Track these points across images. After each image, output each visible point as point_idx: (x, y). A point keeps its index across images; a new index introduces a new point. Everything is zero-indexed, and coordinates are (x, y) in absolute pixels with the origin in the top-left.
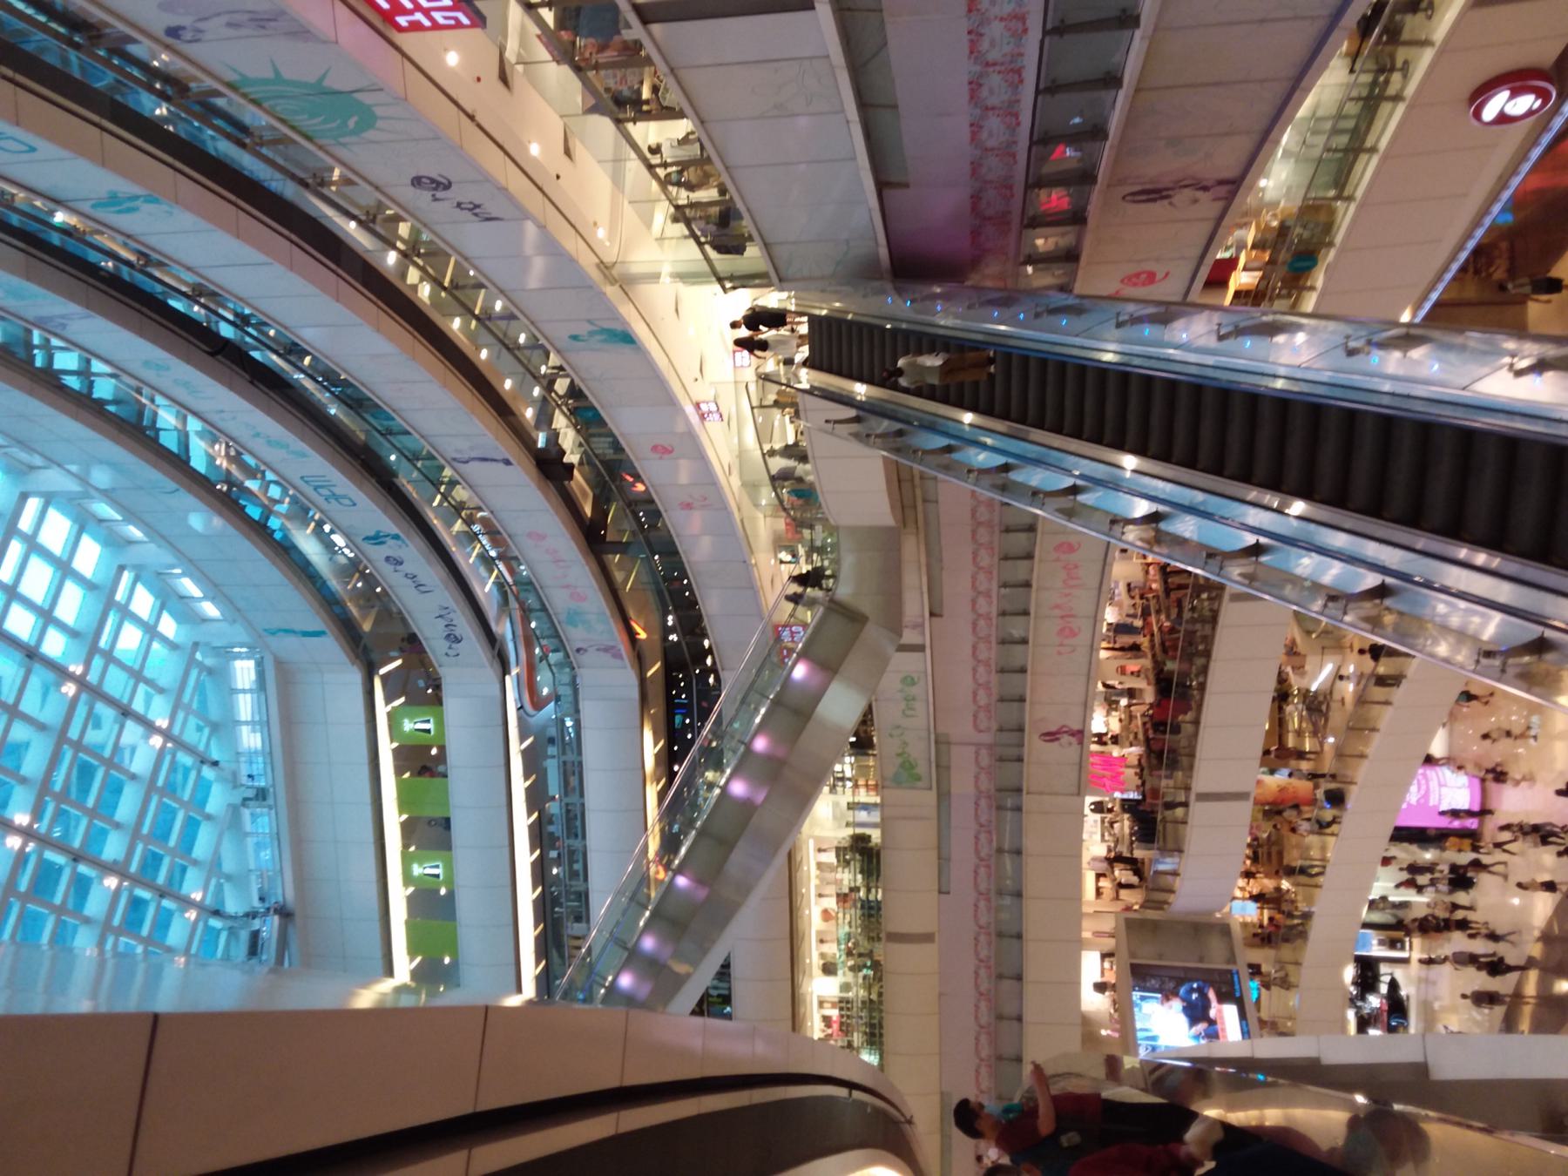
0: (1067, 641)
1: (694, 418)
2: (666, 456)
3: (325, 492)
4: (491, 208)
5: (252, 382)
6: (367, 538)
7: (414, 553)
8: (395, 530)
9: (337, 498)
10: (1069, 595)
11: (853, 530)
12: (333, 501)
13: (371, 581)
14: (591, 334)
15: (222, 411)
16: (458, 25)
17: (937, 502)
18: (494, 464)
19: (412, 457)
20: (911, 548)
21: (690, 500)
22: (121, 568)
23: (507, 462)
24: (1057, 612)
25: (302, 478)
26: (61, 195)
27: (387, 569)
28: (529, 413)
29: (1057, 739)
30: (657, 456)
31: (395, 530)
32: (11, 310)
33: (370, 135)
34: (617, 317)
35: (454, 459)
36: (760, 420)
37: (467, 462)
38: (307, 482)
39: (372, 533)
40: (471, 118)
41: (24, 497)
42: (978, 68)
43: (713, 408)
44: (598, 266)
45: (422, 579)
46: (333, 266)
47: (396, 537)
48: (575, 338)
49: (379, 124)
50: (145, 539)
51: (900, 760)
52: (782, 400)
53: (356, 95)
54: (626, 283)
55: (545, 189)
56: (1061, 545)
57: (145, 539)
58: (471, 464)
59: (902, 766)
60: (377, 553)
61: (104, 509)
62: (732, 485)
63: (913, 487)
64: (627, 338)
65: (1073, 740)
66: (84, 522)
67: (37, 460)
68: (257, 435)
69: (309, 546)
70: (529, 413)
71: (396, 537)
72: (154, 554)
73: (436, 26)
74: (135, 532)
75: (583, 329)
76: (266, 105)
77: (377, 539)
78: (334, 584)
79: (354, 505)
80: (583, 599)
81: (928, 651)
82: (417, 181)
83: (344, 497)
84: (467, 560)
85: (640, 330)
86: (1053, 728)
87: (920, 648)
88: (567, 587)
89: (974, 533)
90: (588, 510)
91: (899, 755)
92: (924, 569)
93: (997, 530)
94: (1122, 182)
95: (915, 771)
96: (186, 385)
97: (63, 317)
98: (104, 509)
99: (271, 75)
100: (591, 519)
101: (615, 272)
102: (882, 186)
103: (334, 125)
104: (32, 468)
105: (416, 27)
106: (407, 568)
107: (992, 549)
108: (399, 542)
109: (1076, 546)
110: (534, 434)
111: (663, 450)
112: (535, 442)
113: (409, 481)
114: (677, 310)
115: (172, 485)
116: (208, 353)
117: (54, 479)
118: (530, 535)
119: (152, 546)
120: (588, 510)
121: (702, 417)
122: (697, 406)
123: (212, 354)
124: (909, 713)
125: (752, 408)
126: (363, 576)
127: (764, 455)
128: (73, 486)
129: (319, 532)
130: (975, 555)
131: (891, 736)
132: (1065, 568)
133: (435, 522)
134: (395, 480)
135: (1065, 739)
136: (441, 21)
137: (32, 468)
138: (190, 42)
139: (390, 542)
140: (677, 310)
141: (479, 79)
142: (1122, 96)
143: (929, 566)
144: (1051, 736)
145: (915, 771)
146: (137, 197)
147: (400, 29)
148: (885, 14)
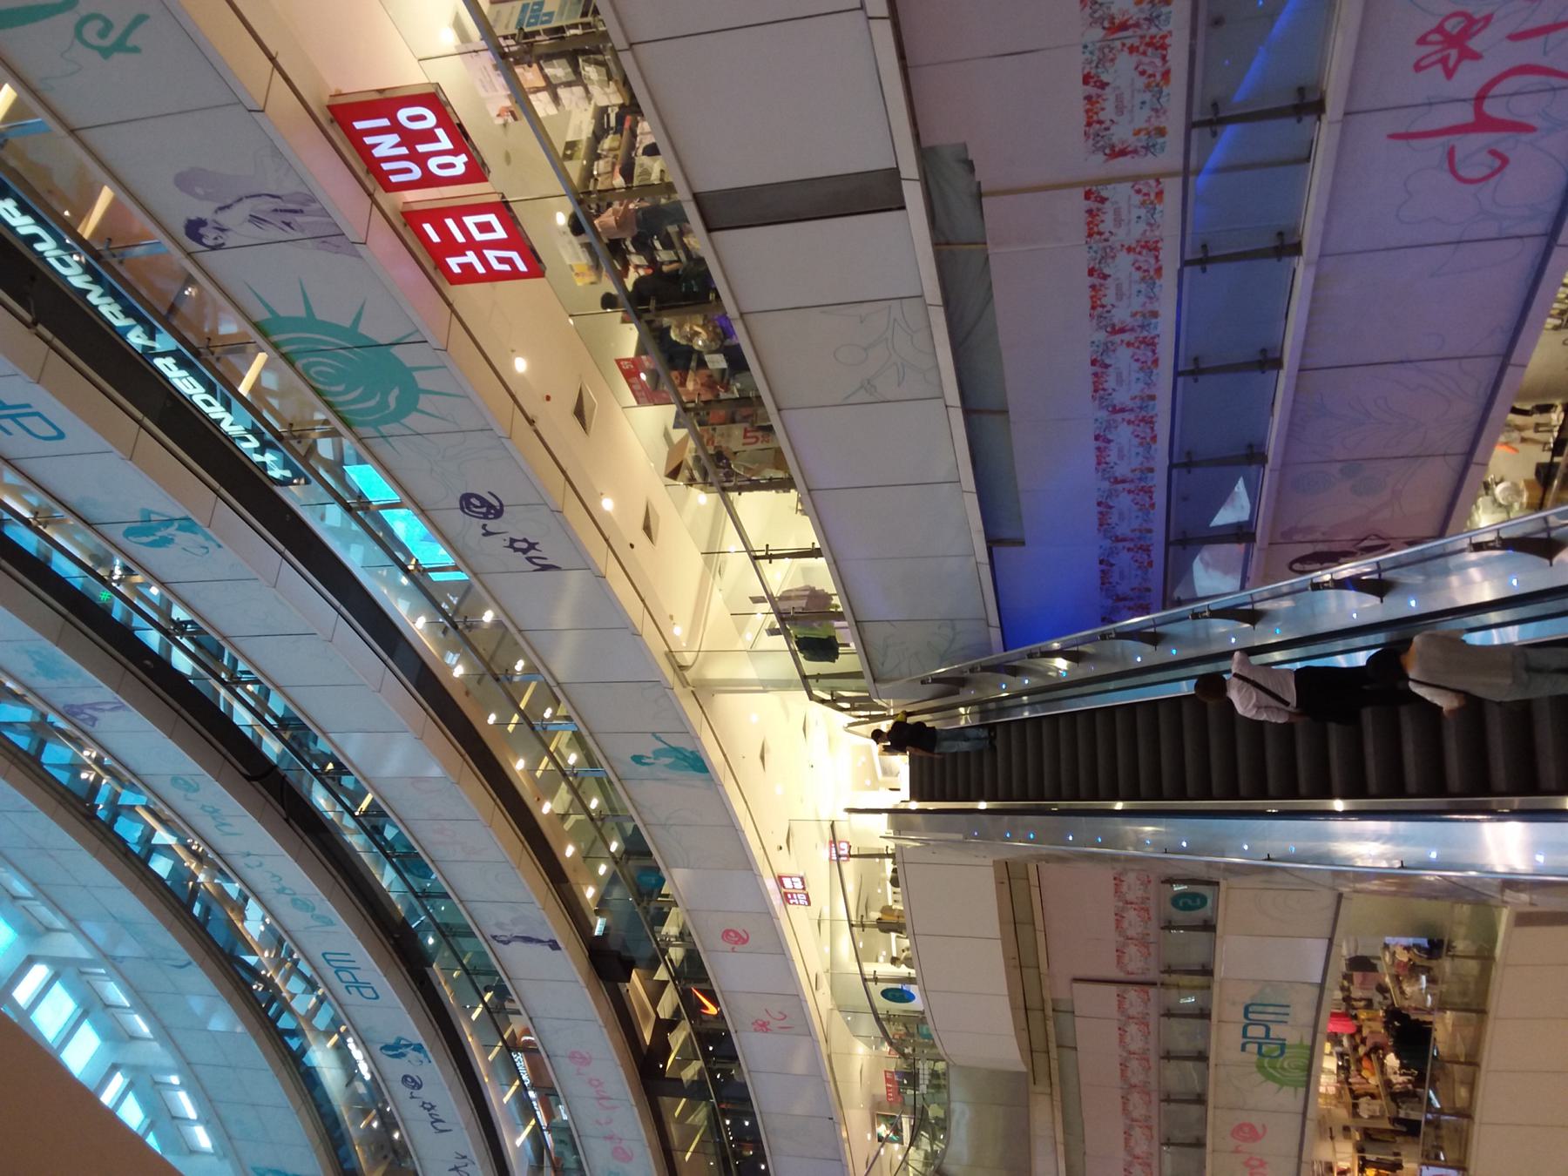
1: (776, 899)
2: (738, 948)
3: (345, 976)
4: (547, 551)
5: (287, 820)
6: (386, 1048)
7: (436, 1075)
8: (418, 1038)
9: (357, 985)
11: (968, 1072)
12: (353, 990)
13: (389, 1123)
14: (658, 754)
15: (249, 855)
16: (515, 274)
17: (1075, 1049)
18: (538, 947)
19: (447, 932)
20: (1044, 1117)
21: (766, 1018)
22: (114, 1068)
23: (554, 946)
25: (324, 955)
26: (94, 514)
27: (402, 1092)
28: (590, 893)
30: (729, 946)
31: (418, 1038)
32: (41, 692)
33: (413, 420)
34: (688, 731)
35: (494, 937)
36: (861, 945)
37: (506, 943)
38: (328, 961)
39: (391, 1041)
40: (531, 422)
41: (30, 961)
42: (1110, 602)
43: (799, 885)
44: (666, 655)
45: (440, 1112)
46: (385, 656)
47: (419, 1048)
48: (638, 759)
49: (424, 402)
50: (151, 1037)
52: (887, 919)
53: (395, 350)
54: (703, 691)
55: (611, 541)
56: (1240, 1127)
57: (151, 1037)
58: (513, 944)
60: (395, 1068)
61: (115, 993)
62: (820, 1002)
63: (1045, 1018)
64: (697, 763)
66: (91, 1007)
67: (59, 923)
68: (281, 891)
69: (321, 1058)
70: (590, 893)
71: (419, 1048)
72: (154, 1052)
73: (492, 276)
74: (141, 1026)
75: (647, 747)
76: (299, 364)
77: (395, 1049)
78: (345, 1115)
79: (377, 997)
80: (627, 1157)
82: (466, 501)
83: (367, 985)
84: (502, 1098)
85: (715, 757)
88: (610, 1138)
89: (1125, 1100)
90: (647, 1036)
92: (1061, 1148)
93: (1155, 1098)
94: (1288, 537)
96: (214, 813)
97: (93, 706)
98: (115, 993)
99: (300, 312)
100: (649, 1048)
101: (689, 675)
102: (992, 542)
103: (372, 403)
104: (49, 930)
105: (468, 274)
106: (424, 1094)
107: (1150, 1128)
108: (421, 1056)
109: (1260, 1131)
110: (592, 921)
111: (736, 938)
112: (592, 928)
113: (471, 1018)
114: (762, 758)
115: (185, 956)
116: (245, 776)
117: (69, 945)
118: (572, 1056)
119: (156, 1046)
120: (647, 1036)
121: (786, 898)
122: (780, 880)
123: (248, 779)
125: (851, 926)
126: (382, 1115)
127: (865, 980)
128: (82, 952)
129: (341, 1048)
130: (1128, 1134)
132: (1247, 1164)
133: (470, 1039)
134: (427, 969)
136: (496, 266)
137: (49, 930)
138: (213, 248)
139: (412, 1054)
140: (762, 758)
141: (548, 398)
142: (1285, 379)
143: (1066, 1145)
146: (171, 520)
147: (454, 279)
148: (989, 245)
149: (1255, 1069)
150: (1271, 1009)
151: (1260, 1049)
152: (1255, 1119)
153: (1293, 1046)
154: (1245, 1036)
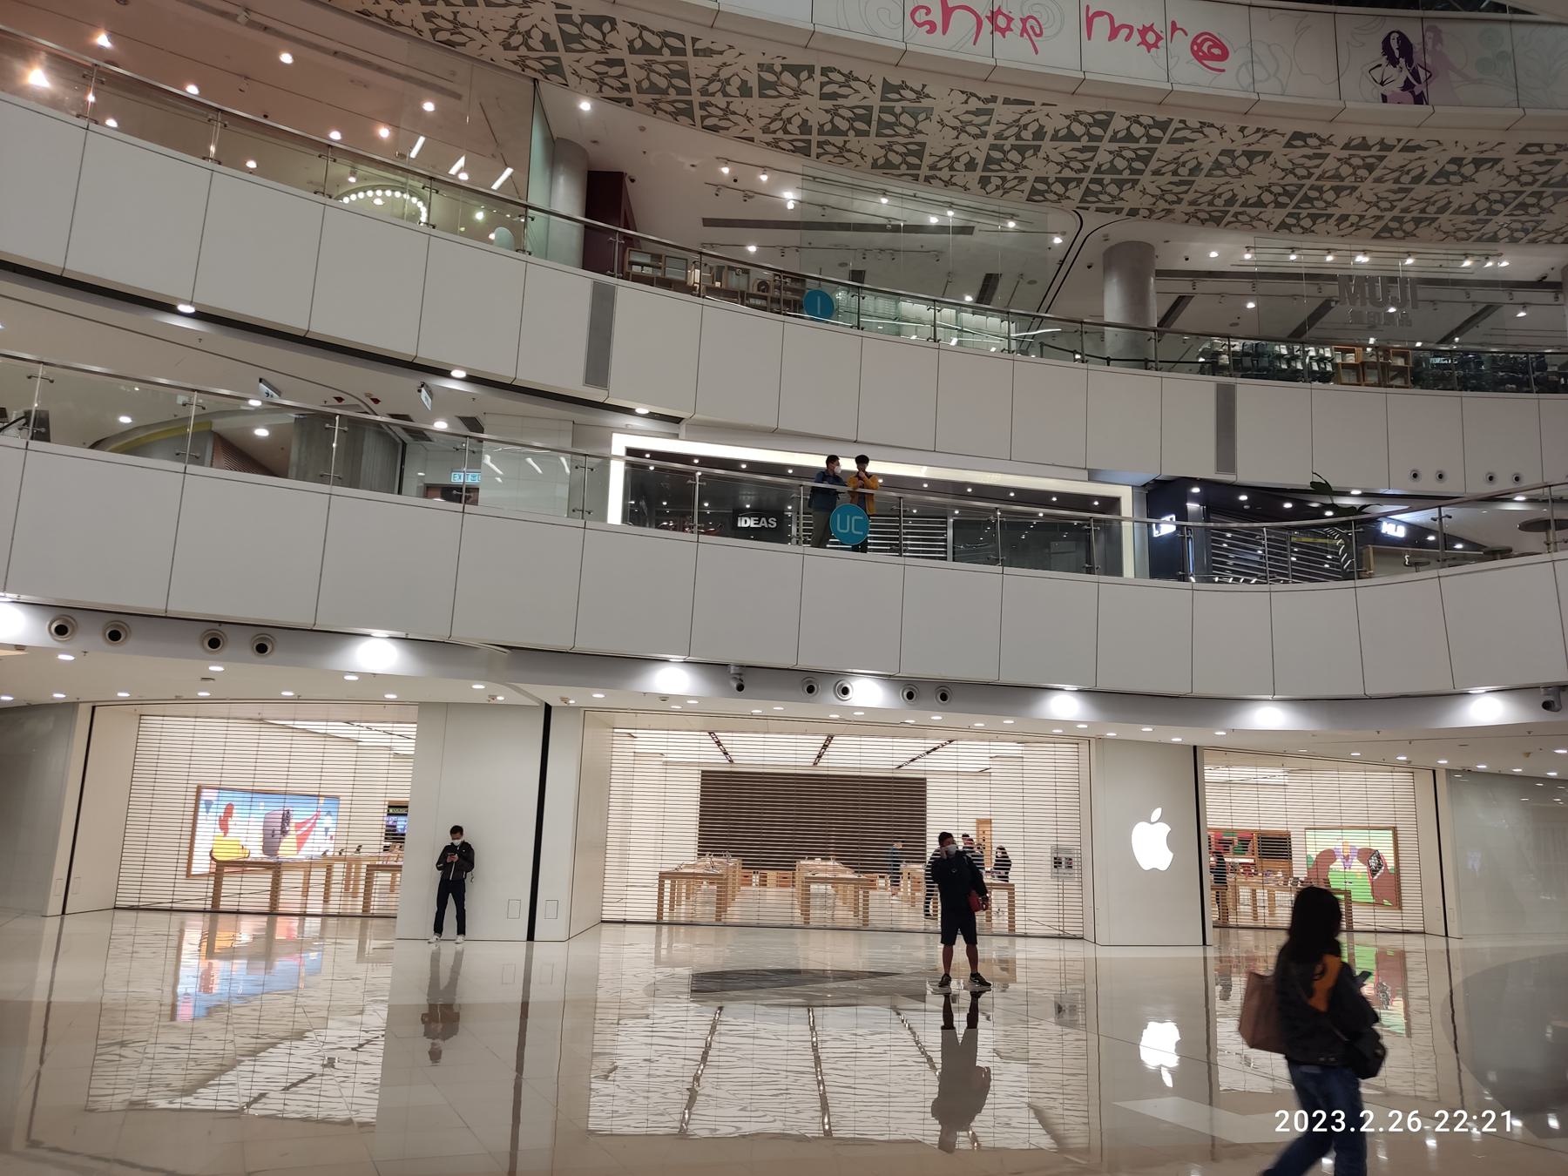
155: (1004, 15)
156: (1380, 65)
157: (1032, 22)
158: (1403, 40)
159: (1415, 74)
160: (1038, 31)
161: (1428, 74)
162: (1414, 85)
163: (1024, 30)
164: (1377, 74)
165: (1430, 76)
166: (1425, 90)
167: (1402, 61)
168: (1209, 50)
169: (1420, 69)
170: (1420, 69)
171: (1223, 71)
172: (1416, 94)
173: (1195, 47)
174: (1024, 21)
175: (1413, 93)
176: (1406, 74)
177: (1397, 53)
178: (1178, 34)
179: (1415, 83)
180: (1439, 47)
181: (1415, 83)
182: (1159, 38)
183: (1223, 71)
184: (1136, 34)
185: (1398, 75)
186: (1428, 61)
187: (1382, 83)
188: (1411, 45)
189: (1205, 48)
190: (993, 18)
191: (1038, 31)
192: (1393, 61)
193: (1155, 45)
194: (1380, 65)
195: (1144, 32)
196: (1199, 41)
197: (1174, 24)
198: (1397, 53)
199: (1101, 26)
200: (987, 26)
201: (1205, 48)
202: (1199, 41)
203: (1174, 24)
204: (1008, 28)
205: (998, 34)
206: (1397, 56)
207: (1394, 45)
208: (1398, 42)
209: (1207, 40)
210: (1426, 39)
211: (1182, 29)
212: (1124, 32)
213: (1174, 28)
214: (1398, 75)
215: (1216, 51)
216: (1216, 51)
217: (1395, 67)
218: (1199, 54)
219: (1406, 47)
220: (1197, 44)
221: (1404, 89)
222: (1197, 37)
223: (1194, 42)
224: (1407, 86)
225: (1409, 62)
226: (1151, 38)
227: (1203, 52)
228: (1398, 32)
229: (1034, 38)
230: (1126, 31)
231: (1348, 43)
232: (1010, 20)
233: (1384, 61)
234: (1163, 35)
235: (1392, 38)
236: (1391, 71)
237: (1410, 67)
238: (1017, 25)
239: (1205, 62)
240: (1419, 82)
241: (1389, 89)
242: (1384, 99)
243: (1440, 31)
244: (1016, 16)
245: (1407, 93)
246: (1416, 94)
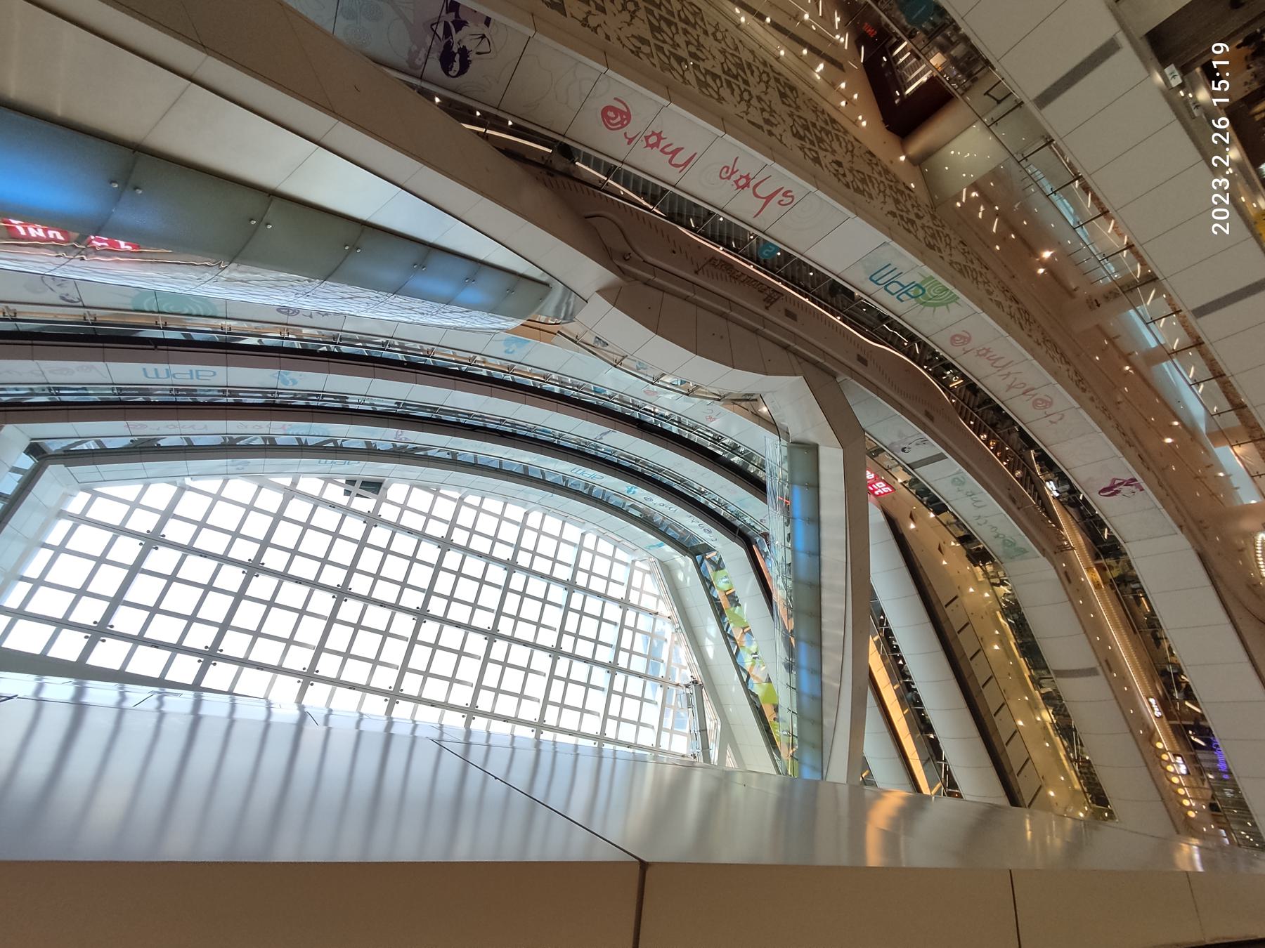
0: (1049, 411)
10: (1009, 374)
24: (1014, 392)
29: (1117, 492)
51: (1000, 541)
59: (1004, 543)
65: (1133, 488)
81: (947, 455)
86: (1107, 485)
87: (940, 457)
91: (997, 537)
95: (1016, 546)
124: (978, 504)
131: (979, 524)
135: (1124, 489)
144: (1111, 490)
145: (1016, 546)
149: (922, 306)
150: (884, 272)
151: (910, 295)
152: (955, 330)
153: (923, 282)
154: (893, 294)
155: (737, 185)
156: (478, 53)
157: (724, 175)
158: (446, 66)
159: (447, 32)
160: (725, 169)
161: (434, 27)
162: (452, 22)
163: (733, 173)
164: (484, 47)
165: (432, 25)
166: (444, 13)
167: (455, 49)
168: (616, 116)
169: (441, 36)
170: (441, 36)
171: (615, 99)
172: (454, 14)
173: (625, 122)
174: (729, 178)
175: (457, 16)
176: (456, 37)
177: (457, 58)
178: (629, 136)
179: (451, 24)
180: (415, 48)
181: (451, 24)
182: (647, 138)
183: (615, 99)
184: (661, 147)
185: (463, 38)
186: (429, 39)
187: (483, 36)
188: (440, 60)
189: (619, 119)
190: (747, 185)
191: (725, 169)
192: (464, 52)
193: (653, 134)
194: (478, 53)
195: (657, 145)
196: (620, 126)
197: (629, 143)
198: (457, 58)
199: (680, 158)
200: (752, 183)
201: (619, 119)
202: (620, 126)
203: (629, 143)
204: (742, 177)
205: (751, 176)
206: (458, 56)
207: (456, 66)
208: (452, 67)
209: (609, 123)
210: (423, 60)
211: (626, 137)
212: (668, 150)
213: (630, 140)
214: (463, 38)
215: (611, 114)
216: (611, 114)
217: (464, 47)
218: (626, 116)
219: (446, 60)
220: (622, 124)
221: (464, 23)
222: (618, 129)
223: (623, 126)
224: (459, 24)
225: (448, 46)
226: (653, 140)
227: (621, 117)
228: (447, 74)
229: (731, 167)
230: (667, 150)
231: (498, 82)
232: (736, 182)
233: (472, 56)
234: (643, 138)
235: (456, 73)
236: (470, 45)
237: (449, 41)
238: (734, 177)
239: (625, 110)
240: (446, 24)
241: (481, 28)
242: (488, 21)
243: (407, 62)
244: (731, 181)
245: (463, 16)
246: (454, 14)
